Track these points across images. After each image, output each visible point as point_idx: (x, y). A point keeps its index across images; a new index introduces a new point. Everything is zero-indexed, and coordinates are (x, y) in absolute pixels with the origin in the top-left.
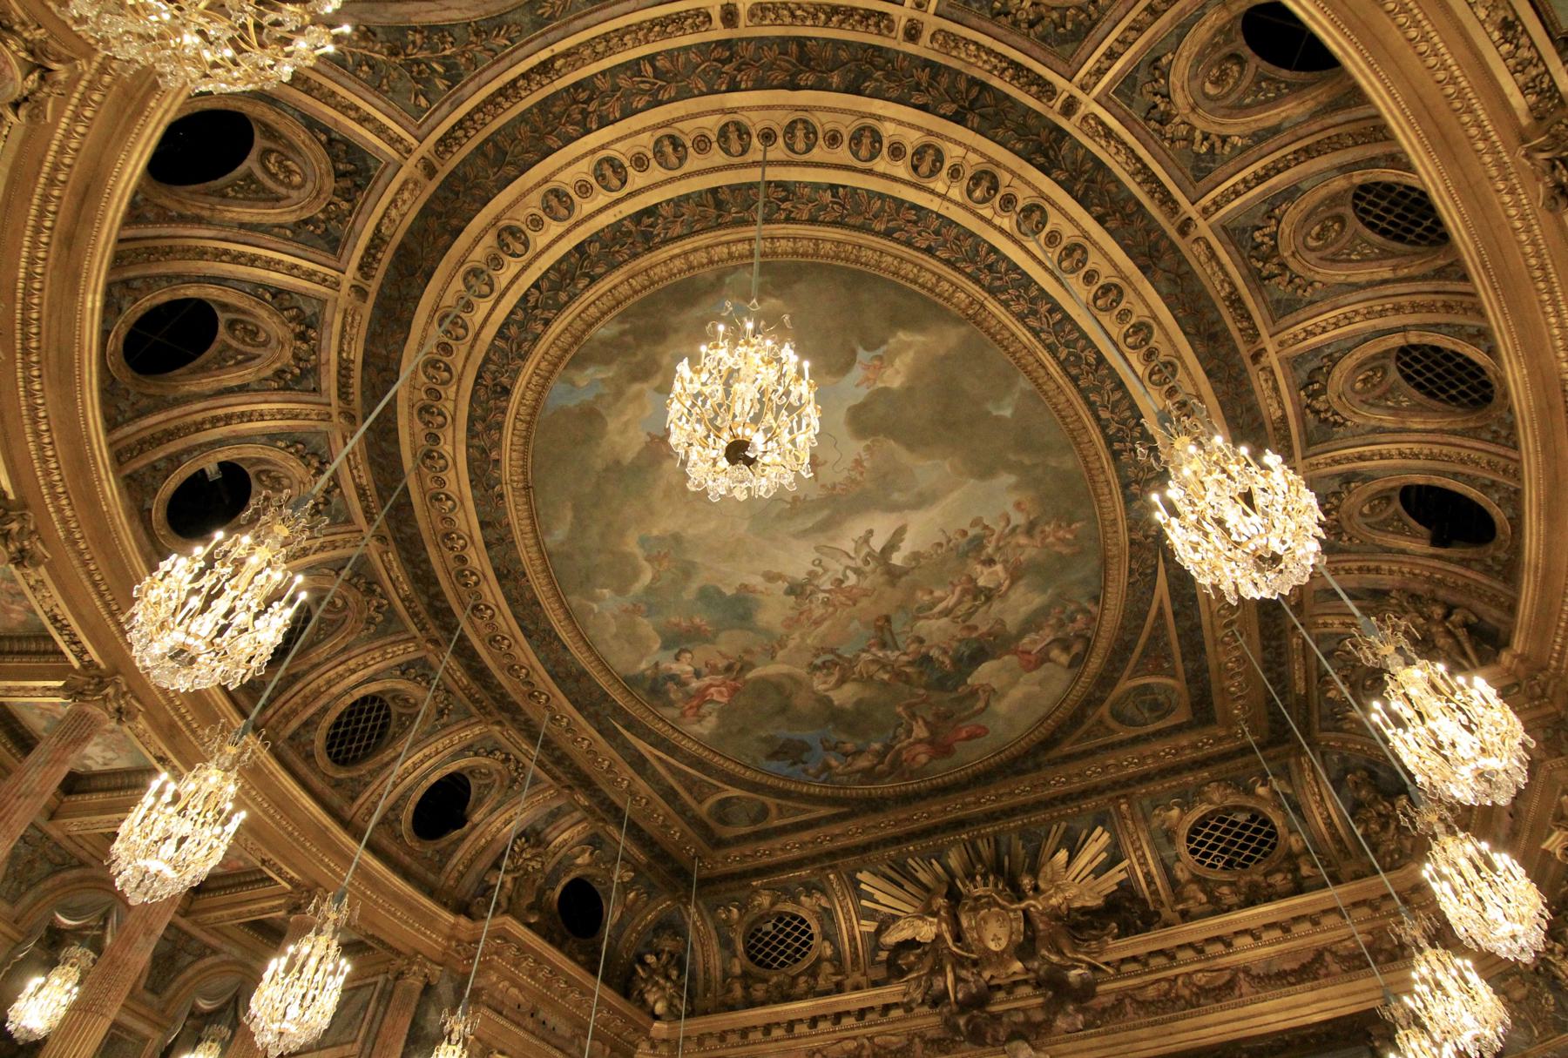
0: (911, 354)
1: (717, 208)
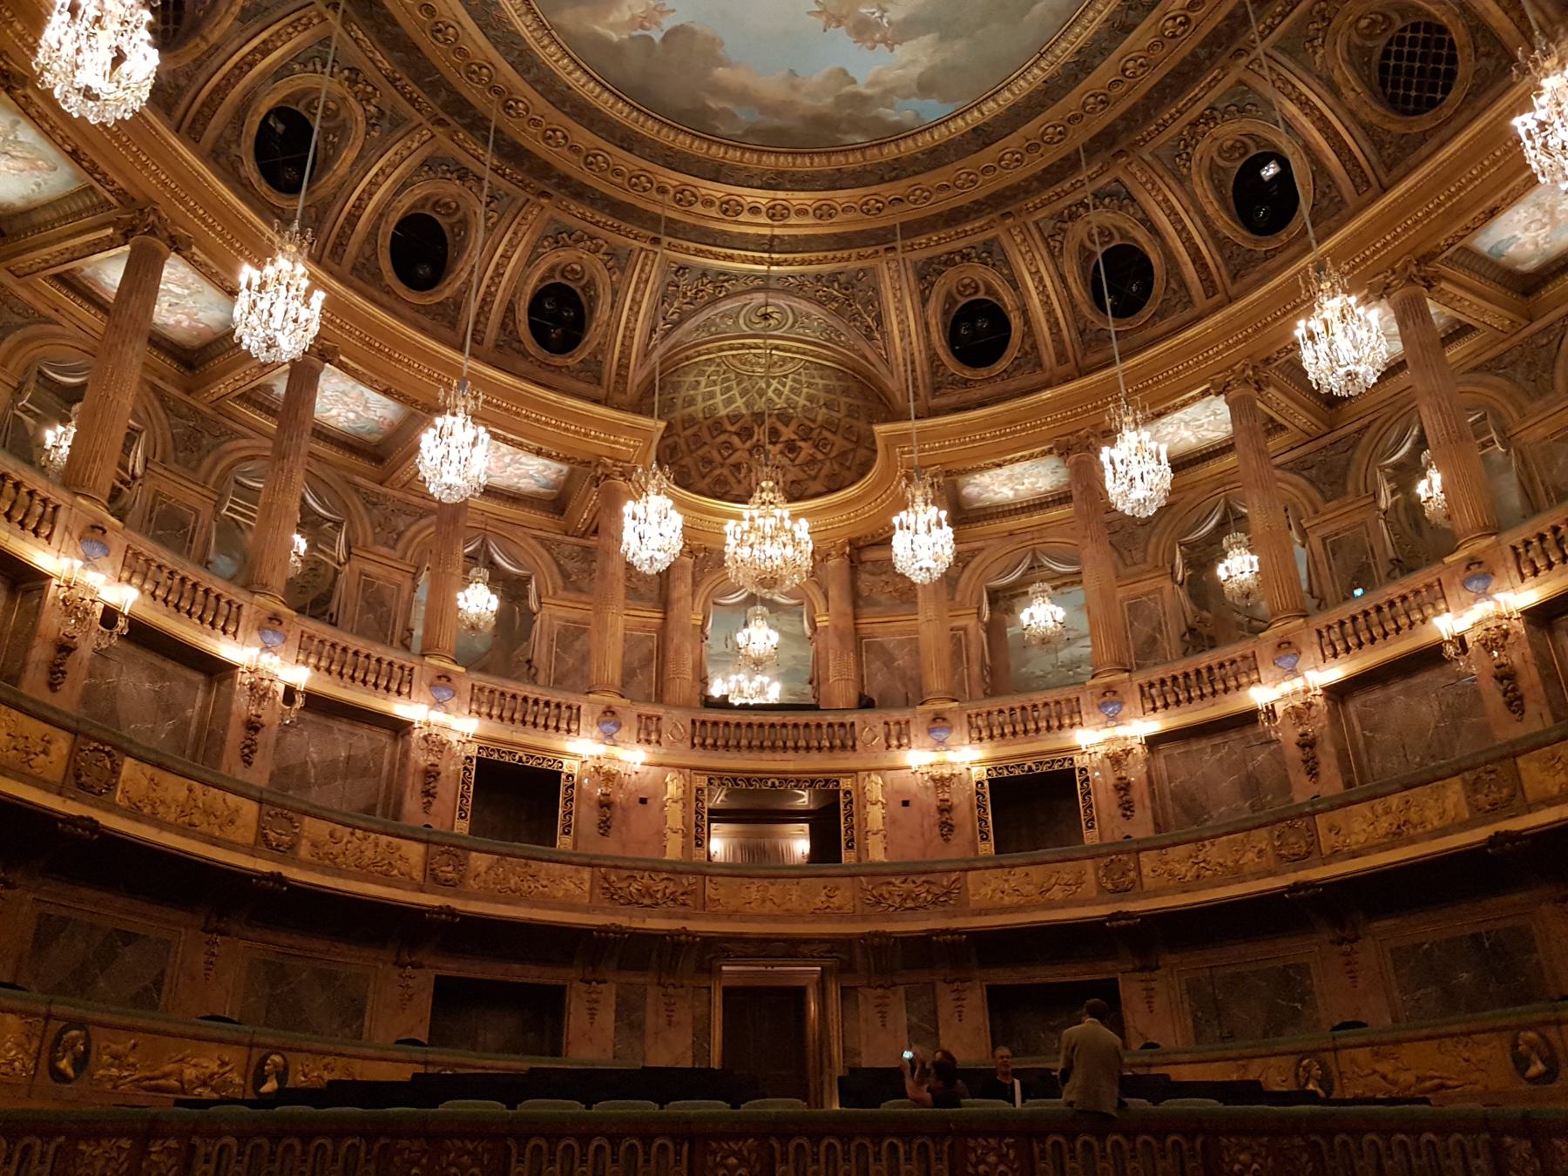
0: (611, 19)
1: (717, 173)
